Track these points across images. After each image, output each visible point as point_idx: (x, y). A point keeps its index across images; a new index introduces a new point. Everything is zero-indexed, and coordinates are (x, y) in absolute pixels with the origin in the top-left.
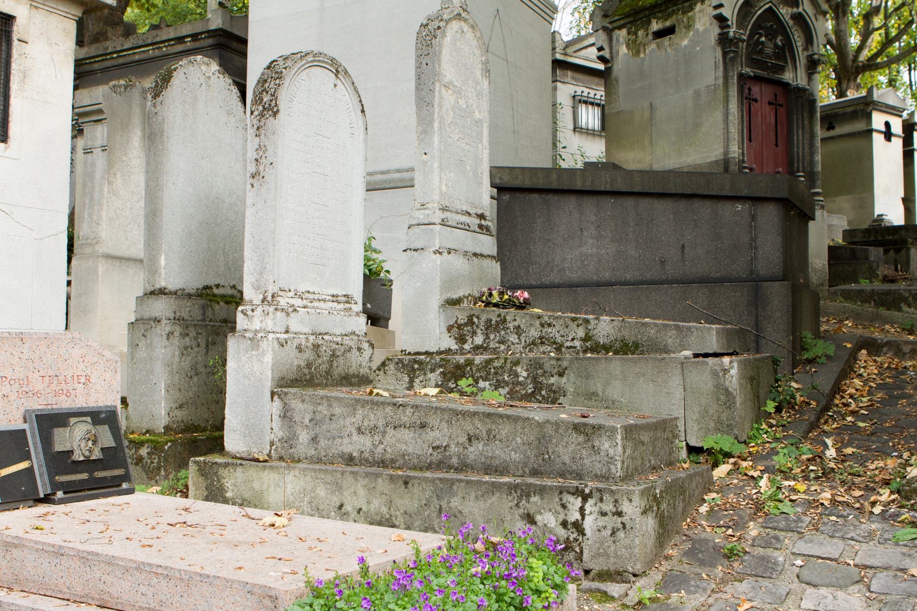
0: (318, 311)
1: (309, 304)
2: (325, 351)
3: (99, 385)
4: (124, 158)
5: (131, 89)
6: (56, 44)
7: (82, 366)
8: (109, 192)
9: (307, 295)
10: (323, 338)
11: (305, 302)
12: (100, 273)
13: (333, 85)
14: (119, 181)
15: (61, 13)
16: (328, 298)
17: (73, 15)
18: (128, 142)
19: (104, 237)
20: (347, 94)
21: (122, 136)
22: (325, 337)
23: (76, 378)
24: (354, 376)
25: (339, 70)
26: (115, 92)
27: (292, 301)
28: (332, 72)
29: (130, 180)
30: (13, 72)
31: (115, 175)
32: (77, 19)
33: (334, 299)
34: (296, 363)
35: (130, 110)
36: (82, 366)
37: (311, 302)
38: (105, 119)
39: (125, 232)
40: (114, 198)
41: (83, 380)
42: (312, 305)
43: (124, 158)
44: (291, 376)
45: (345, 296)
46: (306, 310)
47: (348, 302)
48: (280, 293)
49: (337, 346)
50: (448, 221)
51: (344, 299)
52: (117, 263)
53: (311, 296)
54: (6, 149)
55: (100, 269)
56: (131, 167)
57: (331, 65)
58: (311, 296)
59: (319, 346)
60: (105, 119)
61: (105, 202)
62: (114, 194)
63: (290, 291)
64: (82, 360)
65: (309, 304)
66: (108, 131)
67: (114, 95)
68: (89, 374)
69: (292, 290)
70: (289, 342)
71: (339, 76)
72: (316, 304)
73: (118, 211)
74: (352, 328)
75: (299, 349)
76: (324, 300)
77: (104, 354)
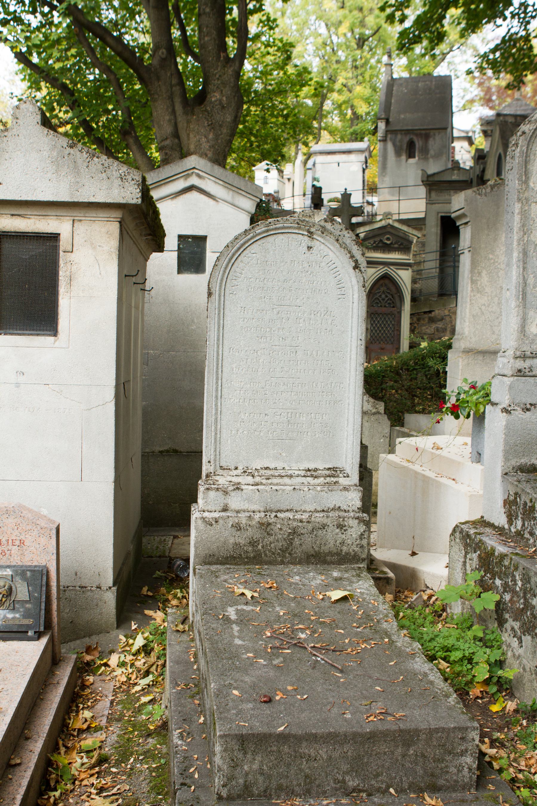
0: (274, 488)
1: (264, 481)
2: (281, 529)
3: (33, 548)
4: (491, 256)
5: (498, 188)
6: (99, 246)
7: (16, 532)
8: (472, 291)
9: (263, 472)
10: (276, 516)
11: (258, 479)
12: (460, 367)
13: (306, 248)
14: (485, 279)
15: (103, 219)
16: (297, 473)
17: (114, 218)
18: (495, 240)
19: (467, 333)
20: (331, 253)
21: (488, 235)
22: (279, 515)
23: (10, 541)
24: (330, 553)
25: (312, 230)
26: (479, 194)
27: (235, 480)
28: (303, 235)
29: (498, 277)
30: (60, 278)
31: (480, 273)
32: (119, 220)
33: (309, 473)
34: (232, 541)
35: (498, 208)
36: (16, 532)
37: (268, 479)
38: (469, 222)
39: (491, 326)
40: (479, 295)
41: (18, 543)
42: (269, 481)
43: (491, 256)
44: (223, 553)
45: (329, 469)
46: (256, 487)
47: (333, 476)
48: (220, 472)
49: (300, 524)
50: (531, 370)
51: (328, 472)
52: (480, 357)
53: (269, 473)
54: (55, 341)
55: (460, 364)
56: (500, 264)
57: (299, 228)
58: (269, 473)
59: (269, 524)
60: (469, 222)
61: (469, 300)
62: (478, 291)
63: (236, 468)
64: (16, 527)
65: (264, 481)
66: (472, 233)
67: (479, 197)
68: (24, 539)
69: (240, 468)
70: (221, 522)
71: (315, 236)
72: (275, 481)
73: (483, 308)
74: (334, 503)
75: (238, 527)
76: (291, 476)
77: (38, 522)
